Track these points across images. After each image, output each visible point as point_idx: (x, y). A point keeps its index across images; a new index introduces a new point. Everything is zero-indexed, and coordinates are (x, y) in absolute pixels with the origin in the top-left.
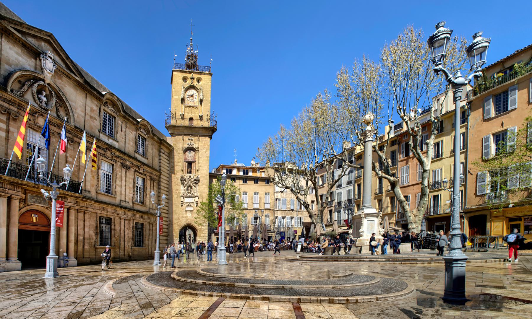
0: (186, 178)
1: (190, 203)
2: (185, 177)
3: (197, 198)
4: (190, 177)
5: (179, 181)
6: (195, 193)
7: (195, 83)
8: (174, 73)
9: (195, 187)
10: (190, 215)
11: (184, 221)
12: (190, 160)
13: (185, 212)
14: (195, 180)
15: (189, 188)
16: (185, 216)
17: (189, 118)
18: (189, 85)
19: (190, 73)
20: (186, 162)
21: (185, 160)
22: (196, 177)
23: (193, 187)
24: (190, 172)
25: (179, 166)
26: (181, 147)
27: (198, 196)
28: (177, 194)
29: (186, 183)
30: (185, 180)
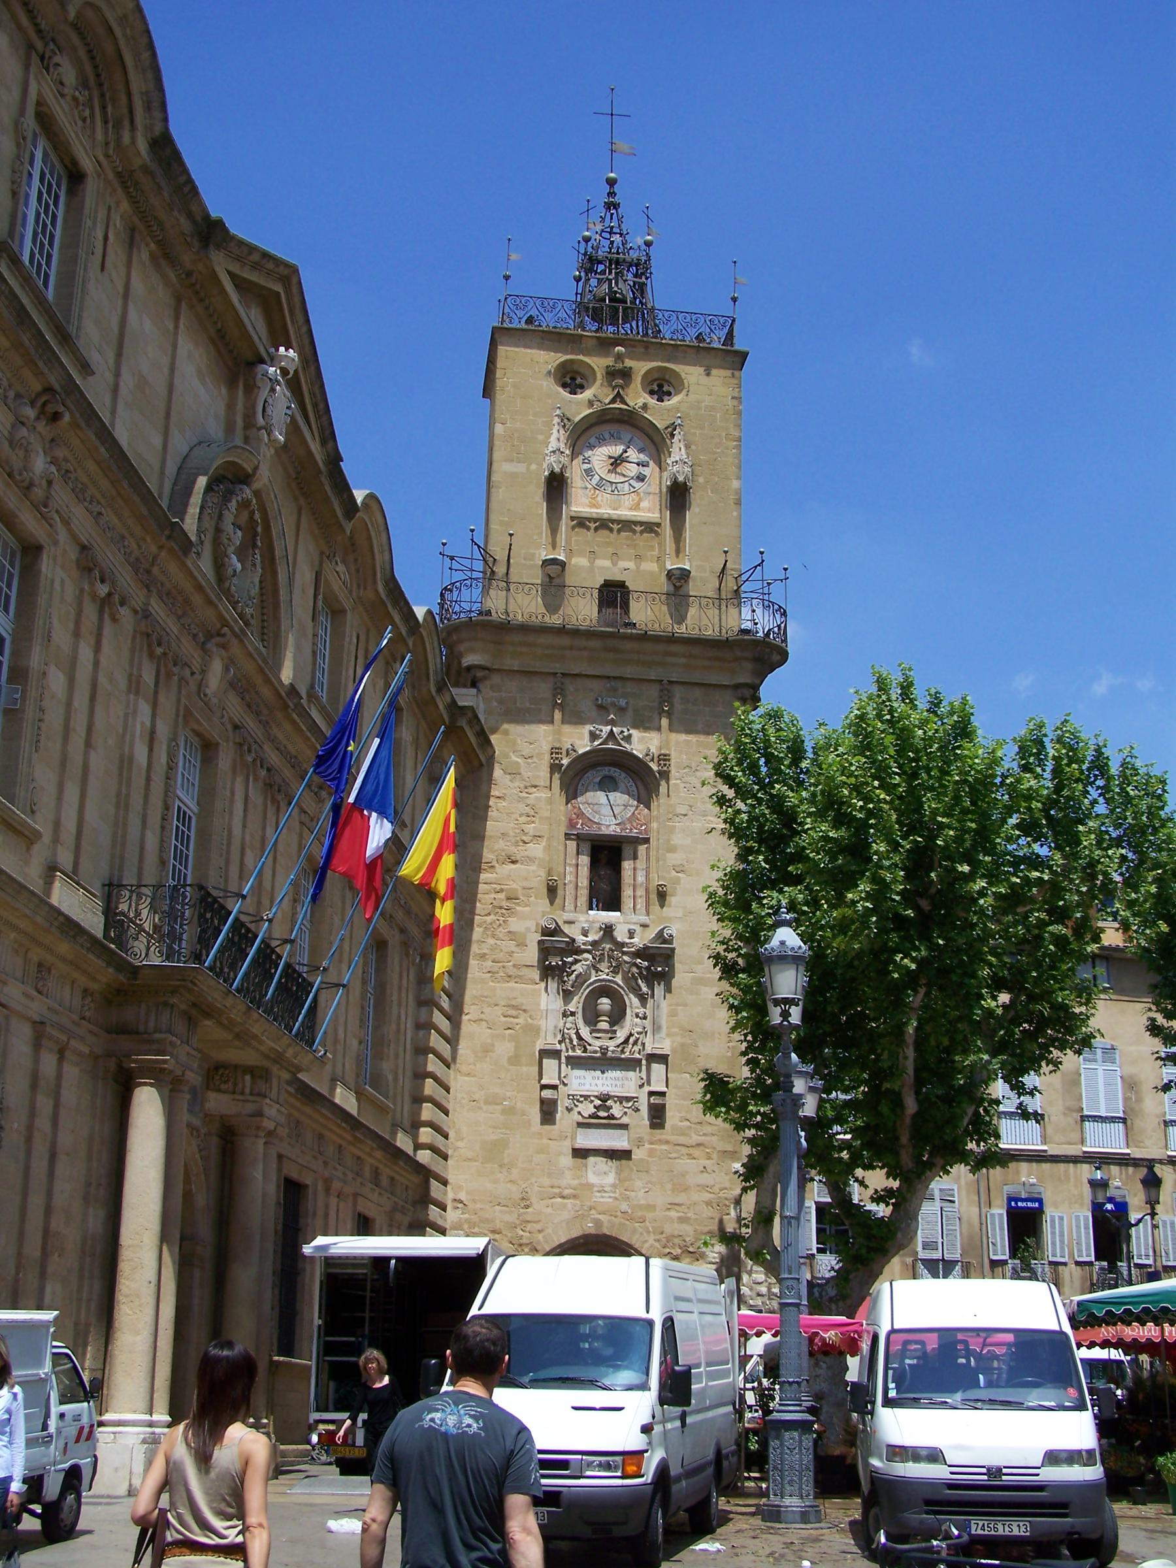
0: (580, 939)
1: (604, 1098)
2: (573, 932)
3: (658, 1069)
4: (608, 930)
5: (532, 954)
6: (648, 1041)
7: (637, 398)
8: (497, 336)
9: (643, 999)
10: (611, 1179)
11: (566, 1215)
12: (609, 826)
13: (567, 1160)
14: (642, 953)
15: (605, 1003)
16: (569, 1180)
17: (600, 581)
18: (597, 407)
19: (605, 345)
20: (579, 838)
21: (571, 824)
22: (651, 933)
23: (632, 1001)
24: (613, 903)
25: (530, 860)
26: (546, 748)
27: (663, 1059)
28: (512, 1038)
29: (579, 968)
30: (572, 948)
